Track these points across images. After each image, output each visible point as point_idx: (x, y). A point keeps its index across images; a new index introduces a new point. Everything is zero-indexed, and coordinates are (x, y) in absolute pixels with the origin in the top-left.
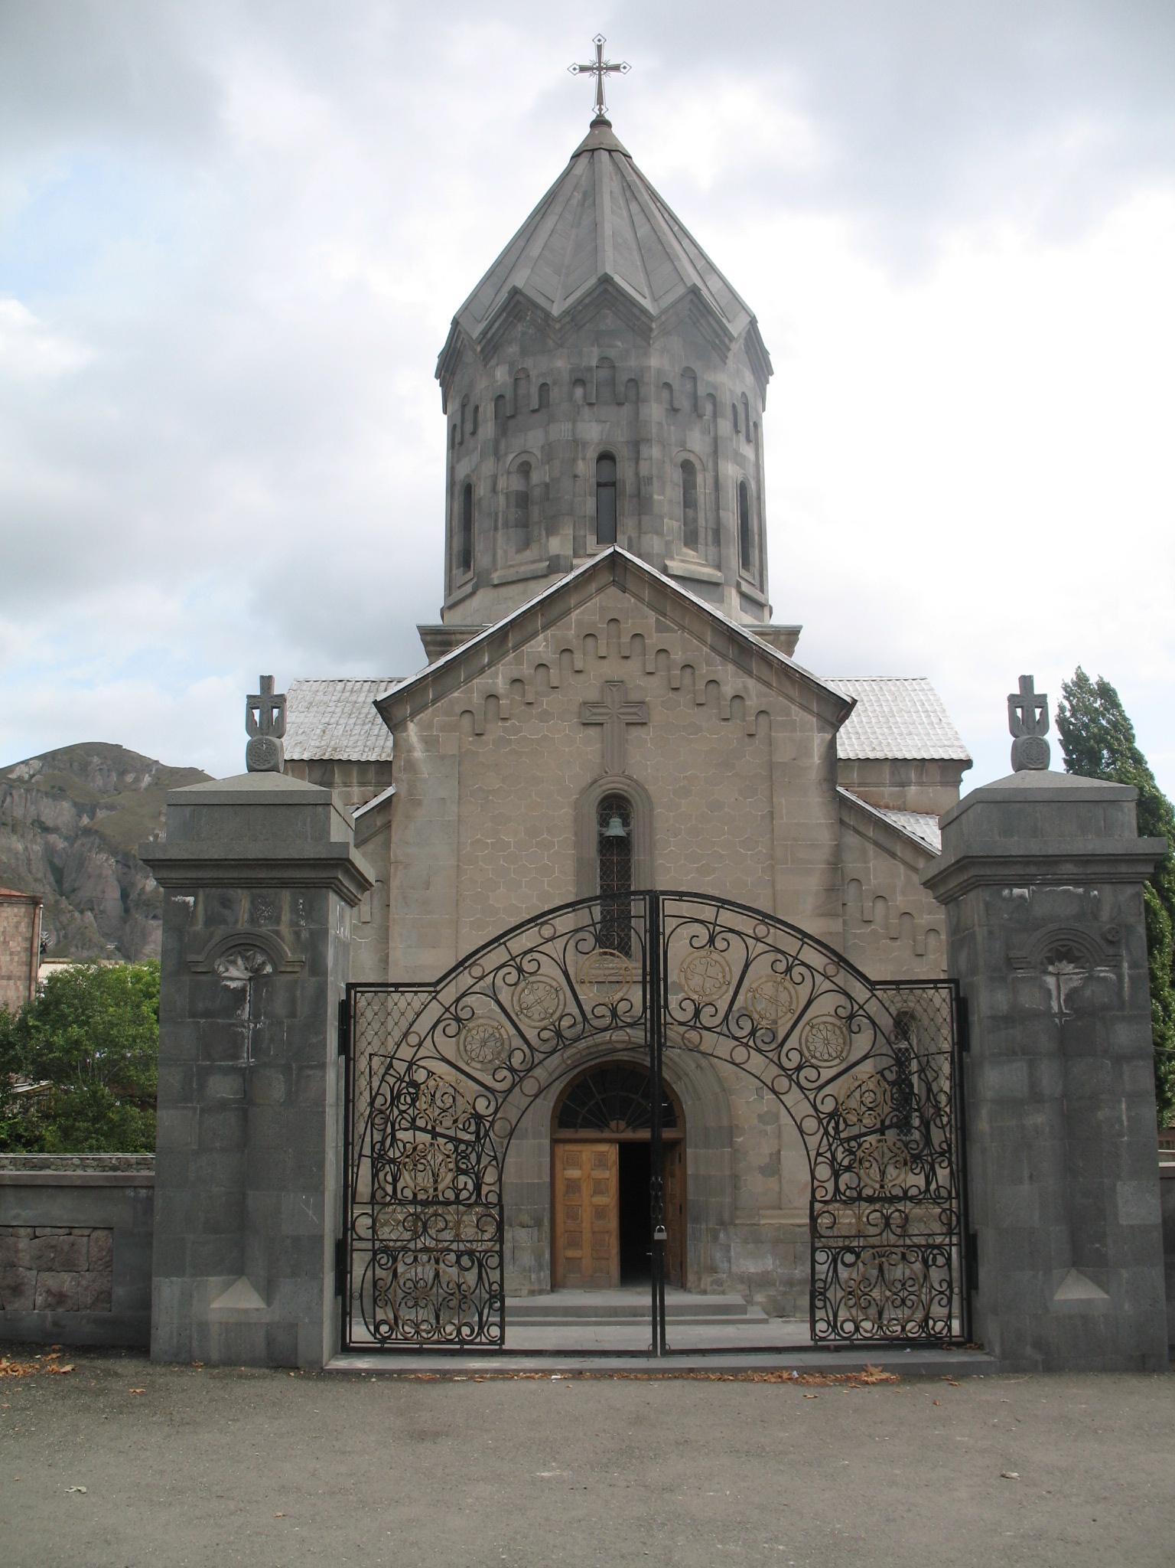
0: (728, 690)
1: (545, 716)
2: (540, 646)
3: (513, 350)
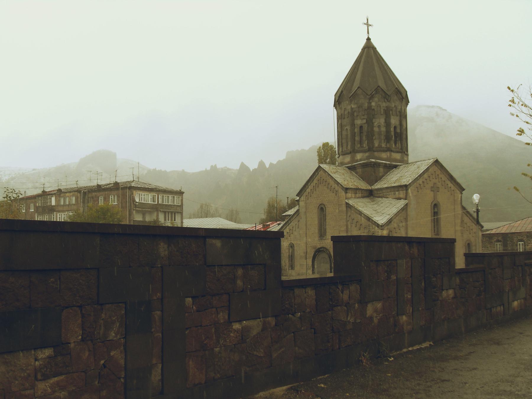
0: (449, 186)
2: (426, 176)
3: (376, 99)
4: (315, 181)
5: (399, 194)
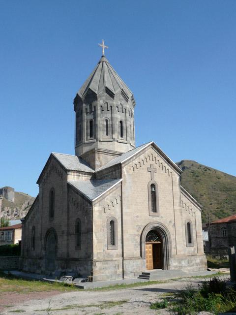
1: (143, 169)
2: (142, 157)
4: (49, 169)
5: (116, 173)
